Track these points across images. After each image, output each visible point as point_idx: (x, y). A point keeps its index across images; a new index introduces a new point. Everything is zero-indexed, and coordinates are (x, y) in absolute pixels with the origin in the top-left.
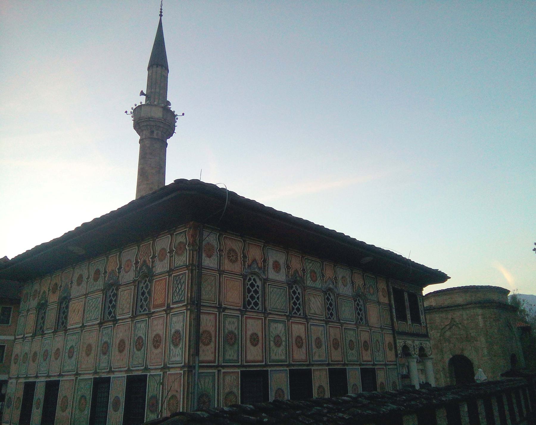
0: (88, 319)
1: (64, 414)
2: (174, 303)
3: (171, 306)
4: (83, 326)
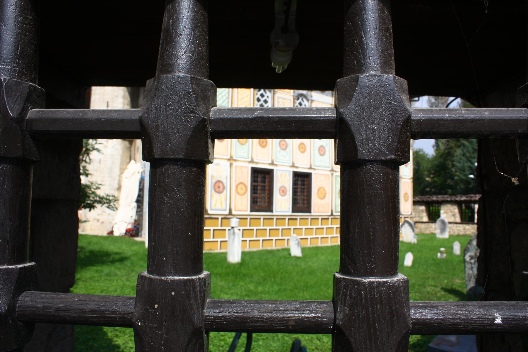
1: (323, 201)
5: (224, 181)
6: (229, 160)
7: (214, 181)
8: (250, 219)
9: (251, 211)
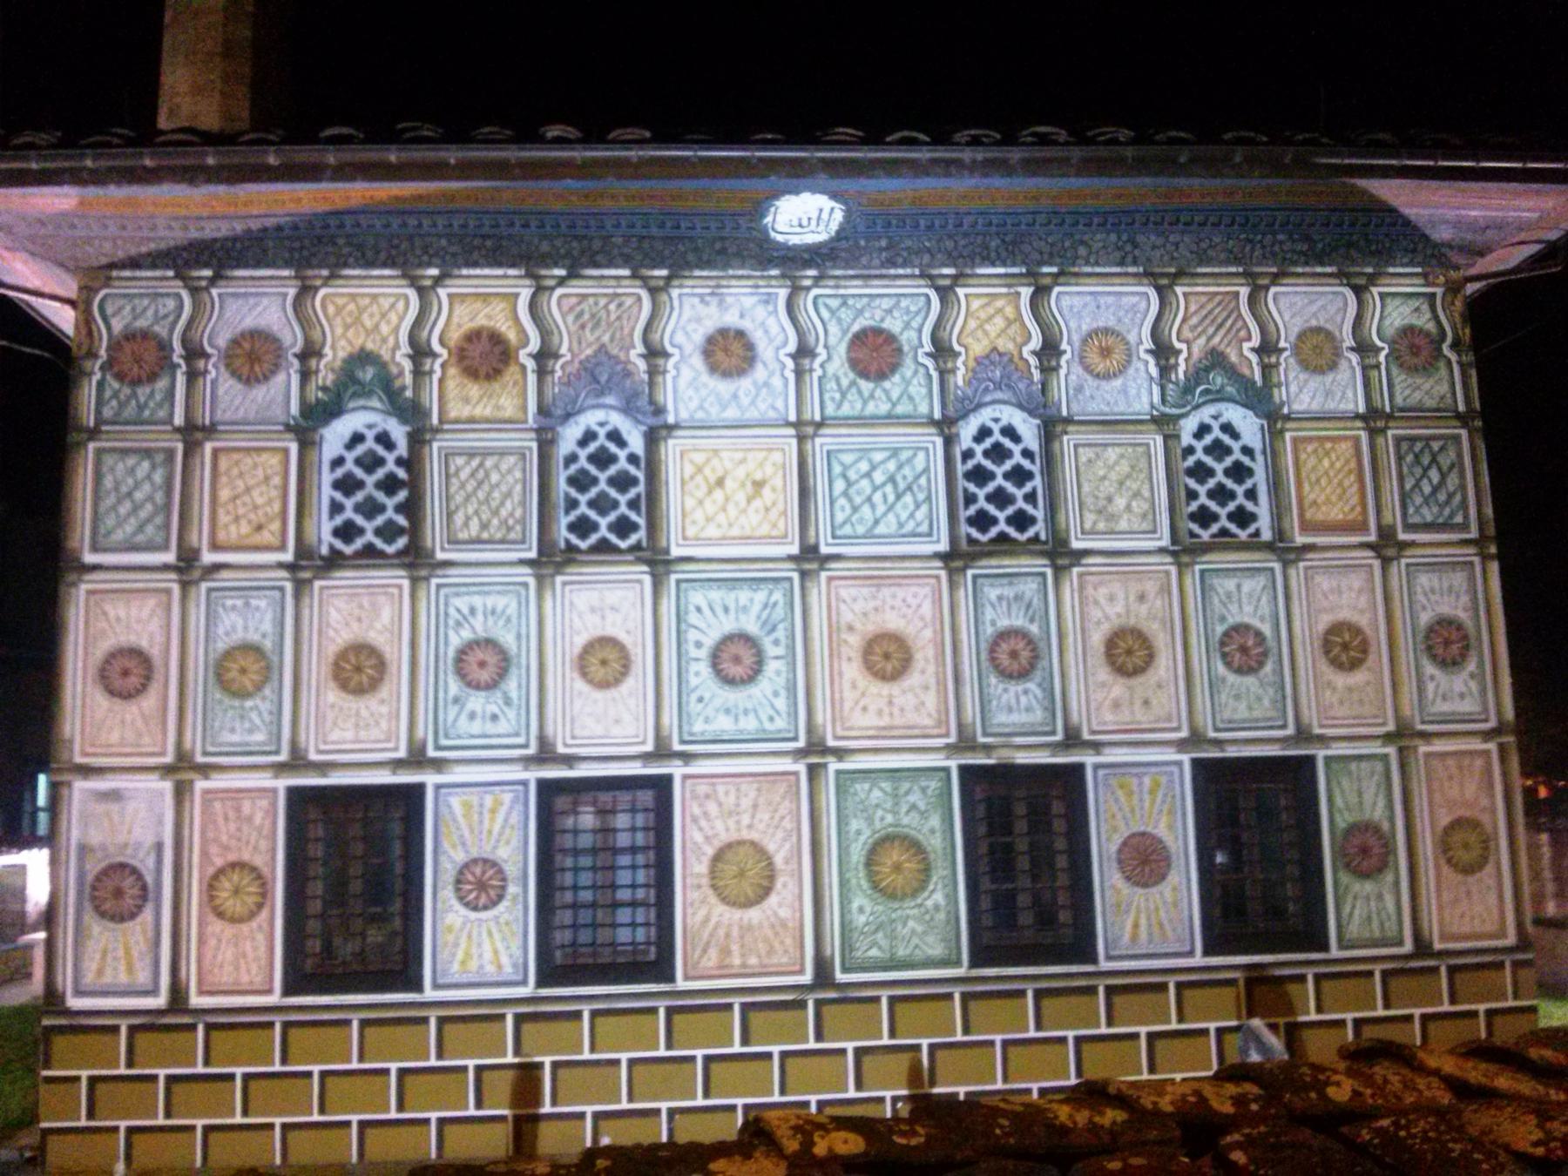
0: (847, 530)
1: (754, 914)
2: (1409, 527)
3: (1402, 536)
4: (809, 557)
5: (147, 866)
6: (166, 771)
7: (93, 867)
8: (287, 1026)
9: (288, 990)
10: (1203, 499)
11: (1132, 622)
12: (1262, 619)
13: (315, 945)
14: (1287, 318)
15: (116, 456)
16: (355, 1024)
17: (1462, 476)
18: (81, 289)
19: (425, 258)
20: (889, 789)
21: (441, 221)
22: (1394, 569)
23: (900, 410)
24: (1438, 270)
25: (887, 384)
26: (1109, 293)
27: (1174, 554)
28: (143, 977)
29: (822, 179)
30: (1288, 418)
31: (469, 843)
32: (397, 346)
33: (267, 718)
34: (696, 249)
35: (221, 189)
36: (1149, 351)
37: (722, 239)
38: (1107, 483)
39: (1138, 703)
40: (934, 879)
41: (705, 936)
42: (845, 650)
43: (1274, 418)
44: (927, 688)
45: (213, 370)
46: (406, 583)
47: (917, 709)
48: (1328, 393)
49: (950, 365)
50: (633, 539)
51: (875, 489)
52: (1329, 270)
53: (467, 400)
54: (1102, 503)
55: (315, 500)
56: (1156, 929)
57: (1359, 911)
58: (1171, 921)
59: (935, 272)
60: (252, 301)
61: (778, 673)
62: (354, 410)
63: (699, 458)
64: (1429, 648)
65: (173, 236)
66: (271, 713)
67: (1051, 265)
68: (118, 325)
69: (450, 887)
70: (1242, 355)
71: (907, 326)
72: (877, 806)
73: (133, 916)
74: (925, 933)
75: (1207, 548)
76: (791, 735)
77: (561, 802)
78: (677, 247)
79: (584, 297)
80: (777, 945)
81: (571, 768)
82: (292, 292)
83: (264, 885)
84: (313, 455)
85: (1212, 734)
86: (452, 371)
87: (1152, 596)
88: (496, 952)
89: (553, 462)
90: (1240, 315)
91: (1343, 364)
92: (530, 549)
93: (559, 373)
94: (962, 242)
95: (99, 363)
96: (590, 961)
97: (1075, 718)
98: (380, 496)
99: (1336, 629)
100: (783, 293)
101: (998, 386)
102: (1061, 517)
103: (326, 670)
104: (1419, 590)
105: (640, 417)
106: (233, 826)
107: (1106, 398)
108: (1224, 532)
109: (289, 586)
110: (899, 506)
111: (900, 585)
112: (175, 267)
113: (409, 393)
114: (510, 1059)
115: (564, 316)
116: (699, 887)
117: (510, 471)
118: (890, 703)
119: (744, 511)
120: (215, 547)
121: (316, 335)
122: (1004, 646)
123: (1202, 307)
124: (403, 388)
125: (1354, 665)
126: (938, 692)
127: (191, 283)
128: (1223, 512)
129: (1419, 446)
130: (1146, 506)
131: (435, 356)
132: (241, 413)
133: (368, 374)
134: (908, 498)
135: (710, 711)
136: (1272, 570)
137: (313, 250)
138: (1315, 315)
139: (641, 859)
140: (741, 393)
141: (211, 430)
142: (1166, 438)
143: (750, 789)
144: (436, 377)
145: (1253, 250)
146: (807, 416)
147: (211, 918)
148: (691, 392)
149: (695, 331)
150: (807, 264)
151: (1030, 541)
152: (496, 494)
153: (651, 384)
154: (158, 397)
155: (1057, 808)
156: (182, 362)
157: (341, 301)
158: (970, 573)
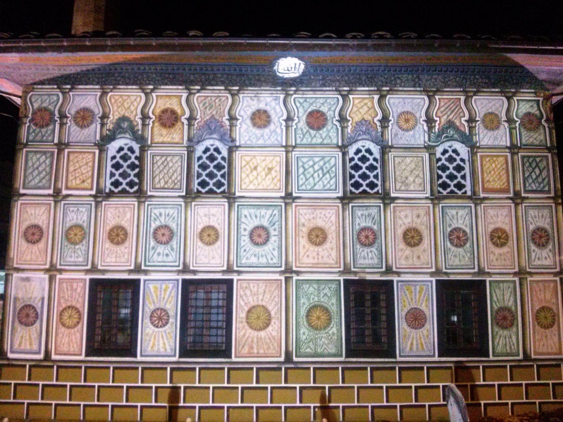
0: (304, 187)
1: (262, 334)
2: (526, 191)
3: (523, 195)
4: (289, 197)
5: (38, 306)
6: (47, 271)
7: (19, 306)
8: (86, 368)
9: (87, 355)
10: (444, 179)
11: (414, 225)
12: (466, 226)
13: (98, 338)
14: (479, 108)
15: (33, 154)
16: (111, 369)
17: (548, 171)
18: (23, 92)
19: (148, 82)
20: (316, 288)
21: (153, 67)
22: (520, 207)
23: (325, 142)
24: (541, 91)
25: (321, 132)
26: (410, 98)
27: (432, 199)
28: (35, 347)
29: (294, 51)
30: (479, 148)
31: (156, 302)
32: (136, 115)
33: (83, 251)
34: (250, 79)
35: (70, 54)
36: (423, 121)
37: (259, 75)
38: (406, 171)
39: (415, 258)
40: (333, 323)
41: (244, 342)
42: (301, 234)
43: (473, 148)
44: (332, 249)
45: (69, 122)
46: (136, 203)
47: (328, 257)
48: (495, 138)
49: (345, 125)
50: (222, 189)
51: (315, 172)
52: (497, 90)
53: (162, 135)
54: (404, 179)
55: (104, 171)
56: (420, 346)
57: (502, 342)
58: (426, 343)
59: (341, 89)
60: (84, 97)
61: (275, 242)
62: (118, 138)
63: (248, 159)
64: (533, 239)
65: (56, 73)
66: (85, 251)
67: (387, 87)
68: (36, 106)
69: (148, 319)
70: (461, 122)
71: (329, 109)
72: (312, 294)
73: (32, 324)
74: (328, 343)
75: (445, 198)
76: (280, 265)
77: (191, 288)
78: (243, 78)
79: (208, 96)
80: (271, 347)
81: (195, 275)
82: (99, 94)
83: (80, 315)
84: (104, 155)
85: (444, 270)
86: (157, 124)
87: (422, 216)
88: (164, 344)
89: (193, 159)
90: (461, 107)
91: (502, 127)
92: (183, 192)
93: (196, 126)
94: (351, 78)
95: (29, 119)
96: (201, 348)
97: (390, 262)
98: (129, 171)
99: (496, 230)
100: (282, 96)
101: (364, 133)
102: (387, 184)
103: (106, 235)
104: (529, 215)
105: (226, 143)
106: (69, 292)
107: (406, 138)
108: (452, 192)
109: (93, 203)
110: (324, 178)
111: (323, 209)
112: (57, 84)
113: (140, 132)
114: (168, 384)
115: (199, 104)
116: (242, 322)
117: (176, 162)
118: (318, 254)
119: (264, 179)
120: (67, 188)
121: (107, 110)
122: (363, 234)
123: (446, 104)
124: (138, 130)
125: (503, 245)
126: (337, 251)
127: (63, 90)
128: (452, 184)
129: (531, 160)
130: (421, 181)
131: (150, 118)
132: (78, 139)
133: (125, 125)
134: (328, 176)
135: (248, 255)
136: (471, 207)
137: (107, 78)
138: (491, 108)
139: (220, 311)
140: (265, 135)
141: (67, 145)
142: (430, 154)
143: (262, 286)
144: (150, 126)
145: (466, 82)
146: (290, 144)
147: (61, 326)
148: (245, 134)
149: (248, 110)
150: (291, 85)
151: (375, 193)
152: (171, 171)
153: (231, 130)
154: (49, 132)
155: (383, 297)
156: (58, 119)
157: (116, 98)
158: (351, 205)
